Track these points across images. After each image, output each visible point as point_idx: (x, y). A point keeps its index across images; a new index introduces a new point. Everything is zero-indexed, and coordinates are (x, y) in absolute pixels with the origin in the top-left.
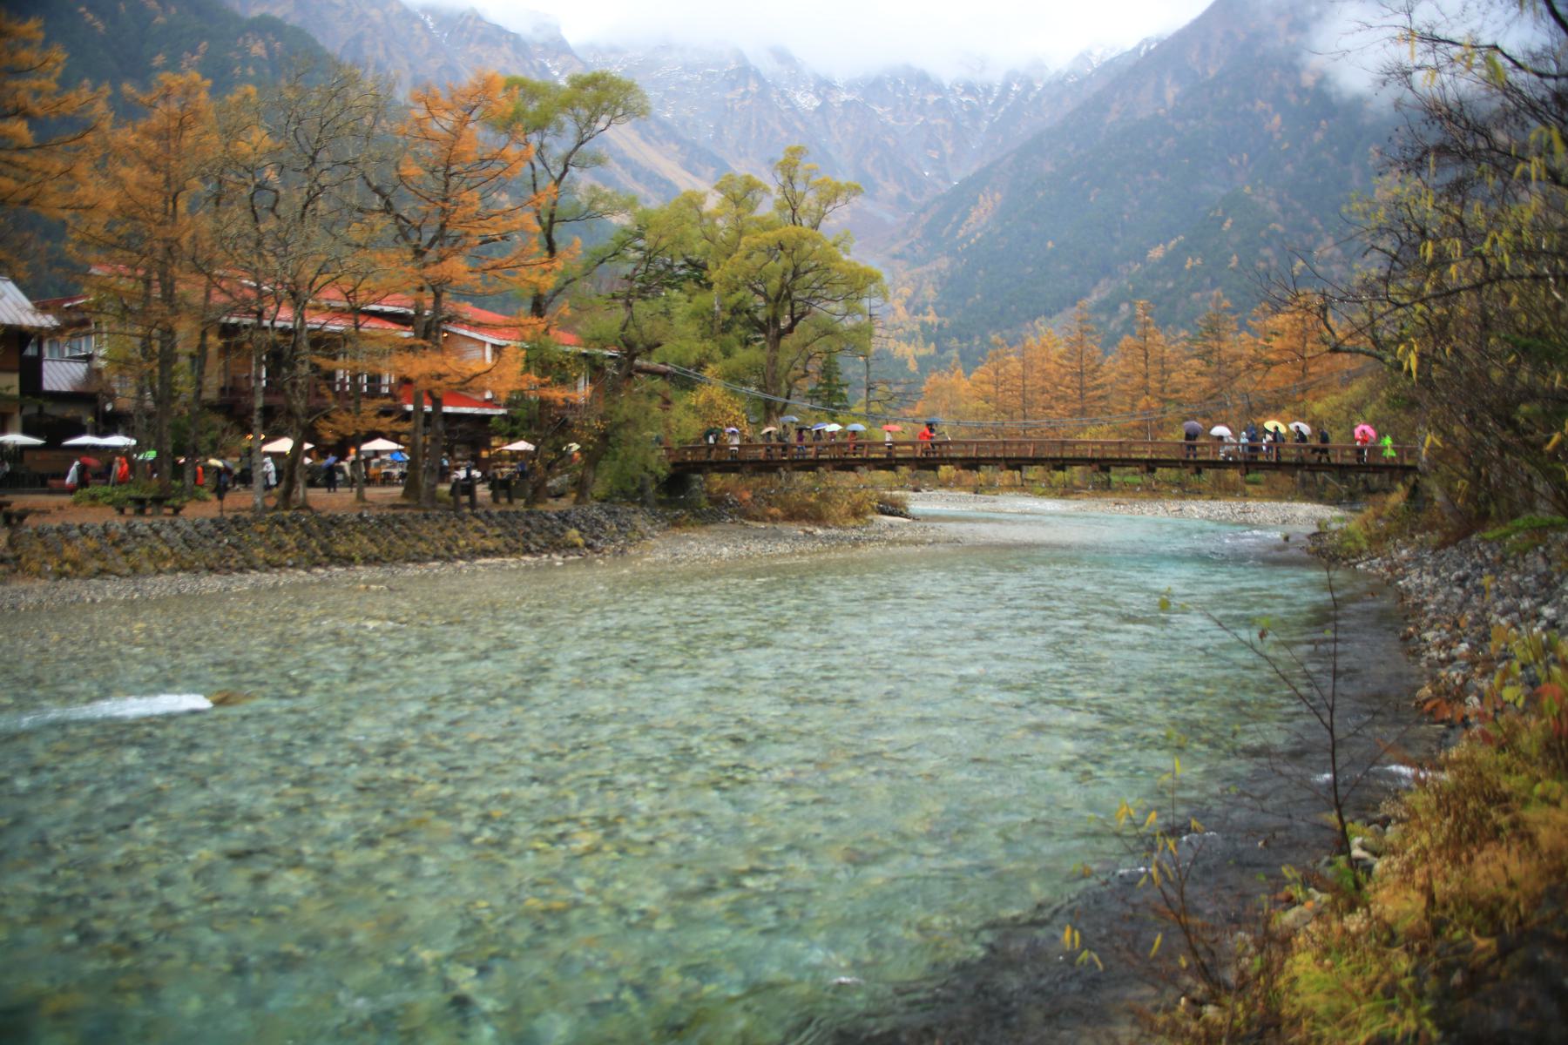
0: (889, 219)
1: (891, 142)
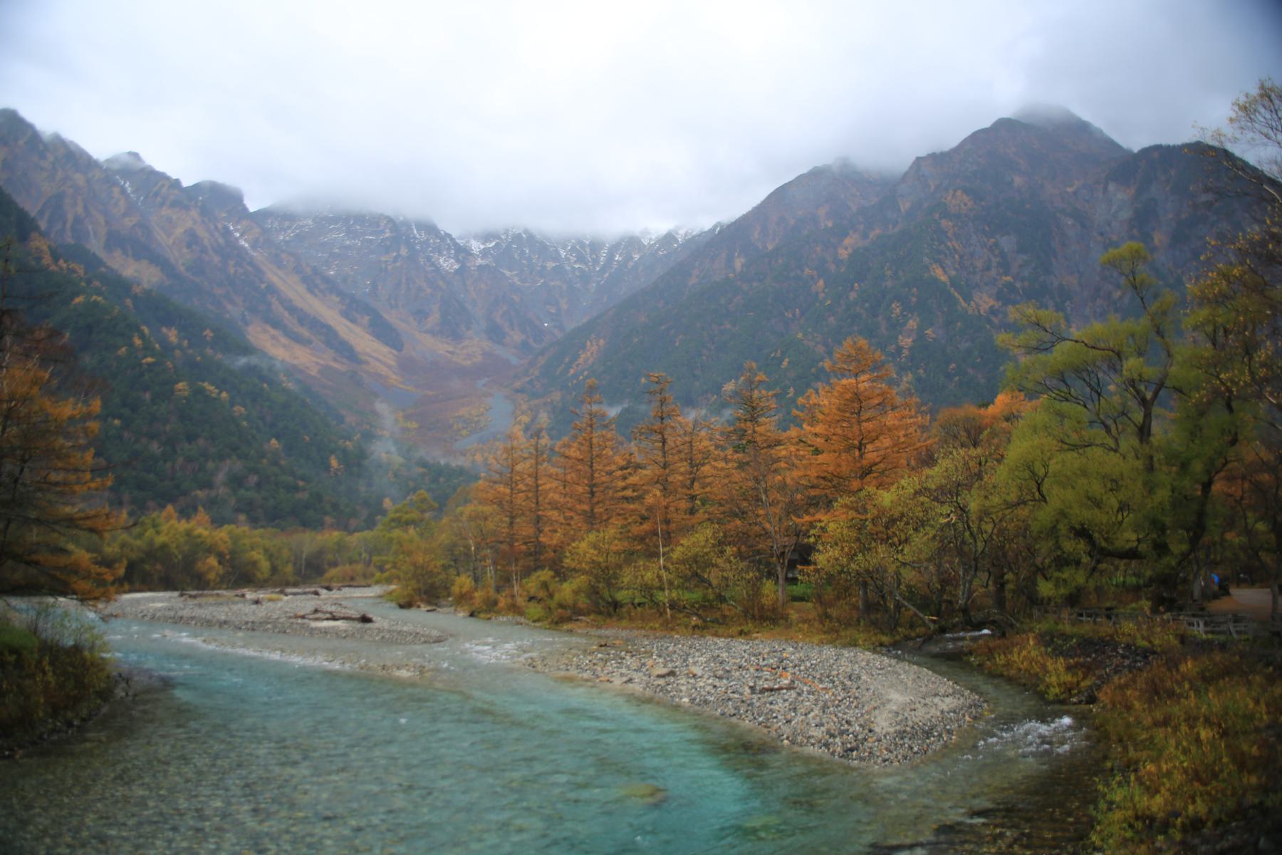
0: (514, 360)
1: (517, 299)
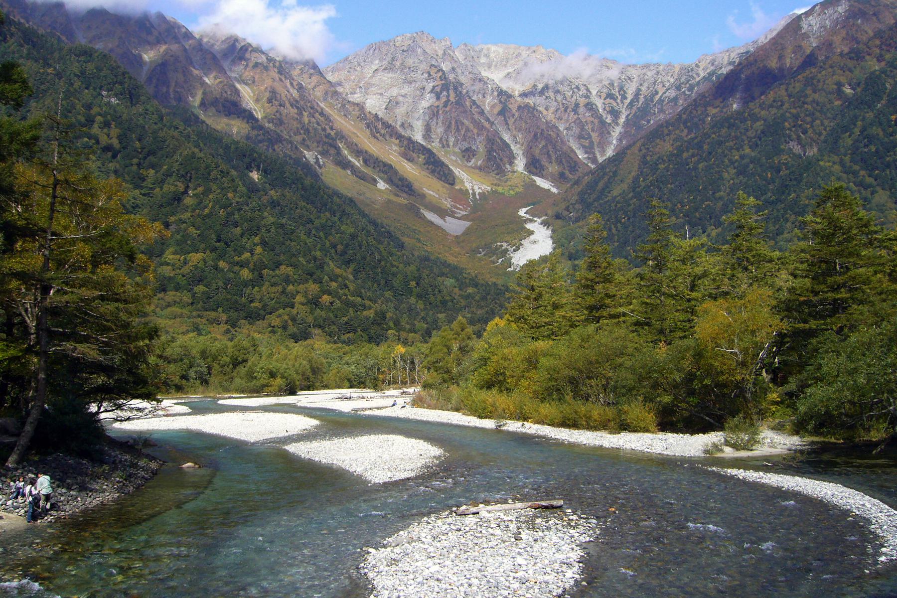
0: (554, 190)
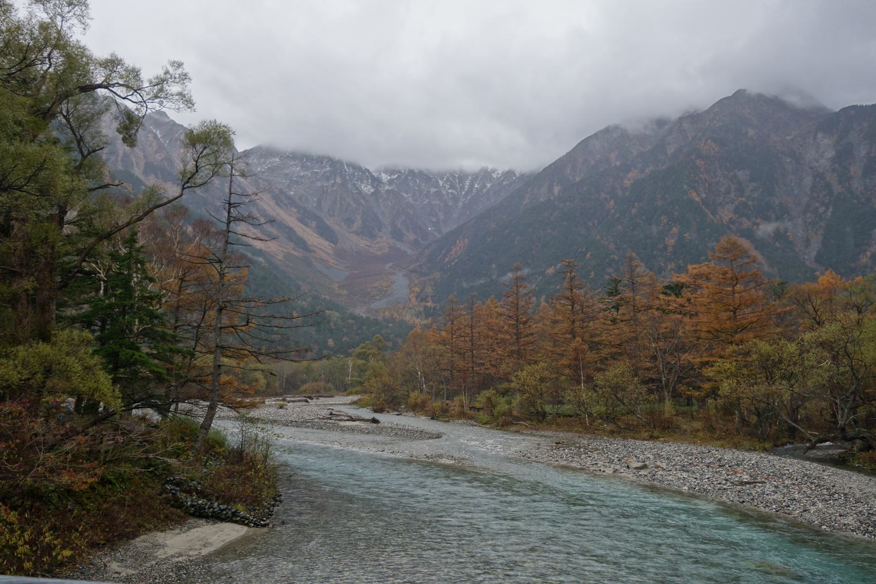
0: (409, 252)
